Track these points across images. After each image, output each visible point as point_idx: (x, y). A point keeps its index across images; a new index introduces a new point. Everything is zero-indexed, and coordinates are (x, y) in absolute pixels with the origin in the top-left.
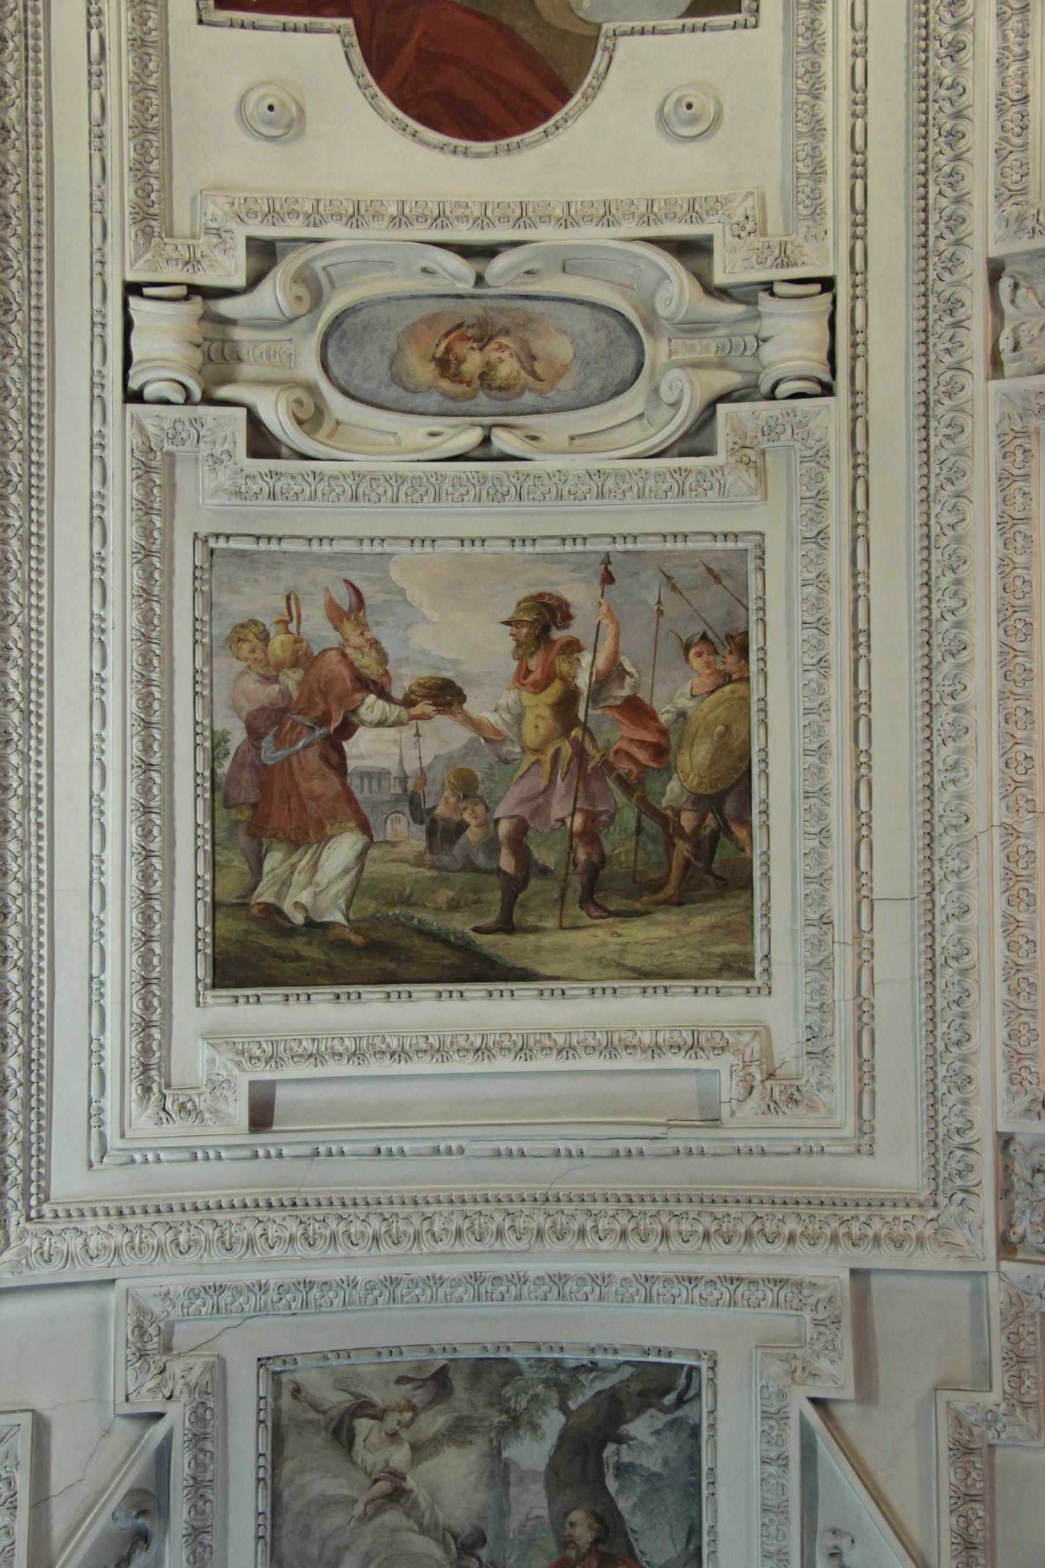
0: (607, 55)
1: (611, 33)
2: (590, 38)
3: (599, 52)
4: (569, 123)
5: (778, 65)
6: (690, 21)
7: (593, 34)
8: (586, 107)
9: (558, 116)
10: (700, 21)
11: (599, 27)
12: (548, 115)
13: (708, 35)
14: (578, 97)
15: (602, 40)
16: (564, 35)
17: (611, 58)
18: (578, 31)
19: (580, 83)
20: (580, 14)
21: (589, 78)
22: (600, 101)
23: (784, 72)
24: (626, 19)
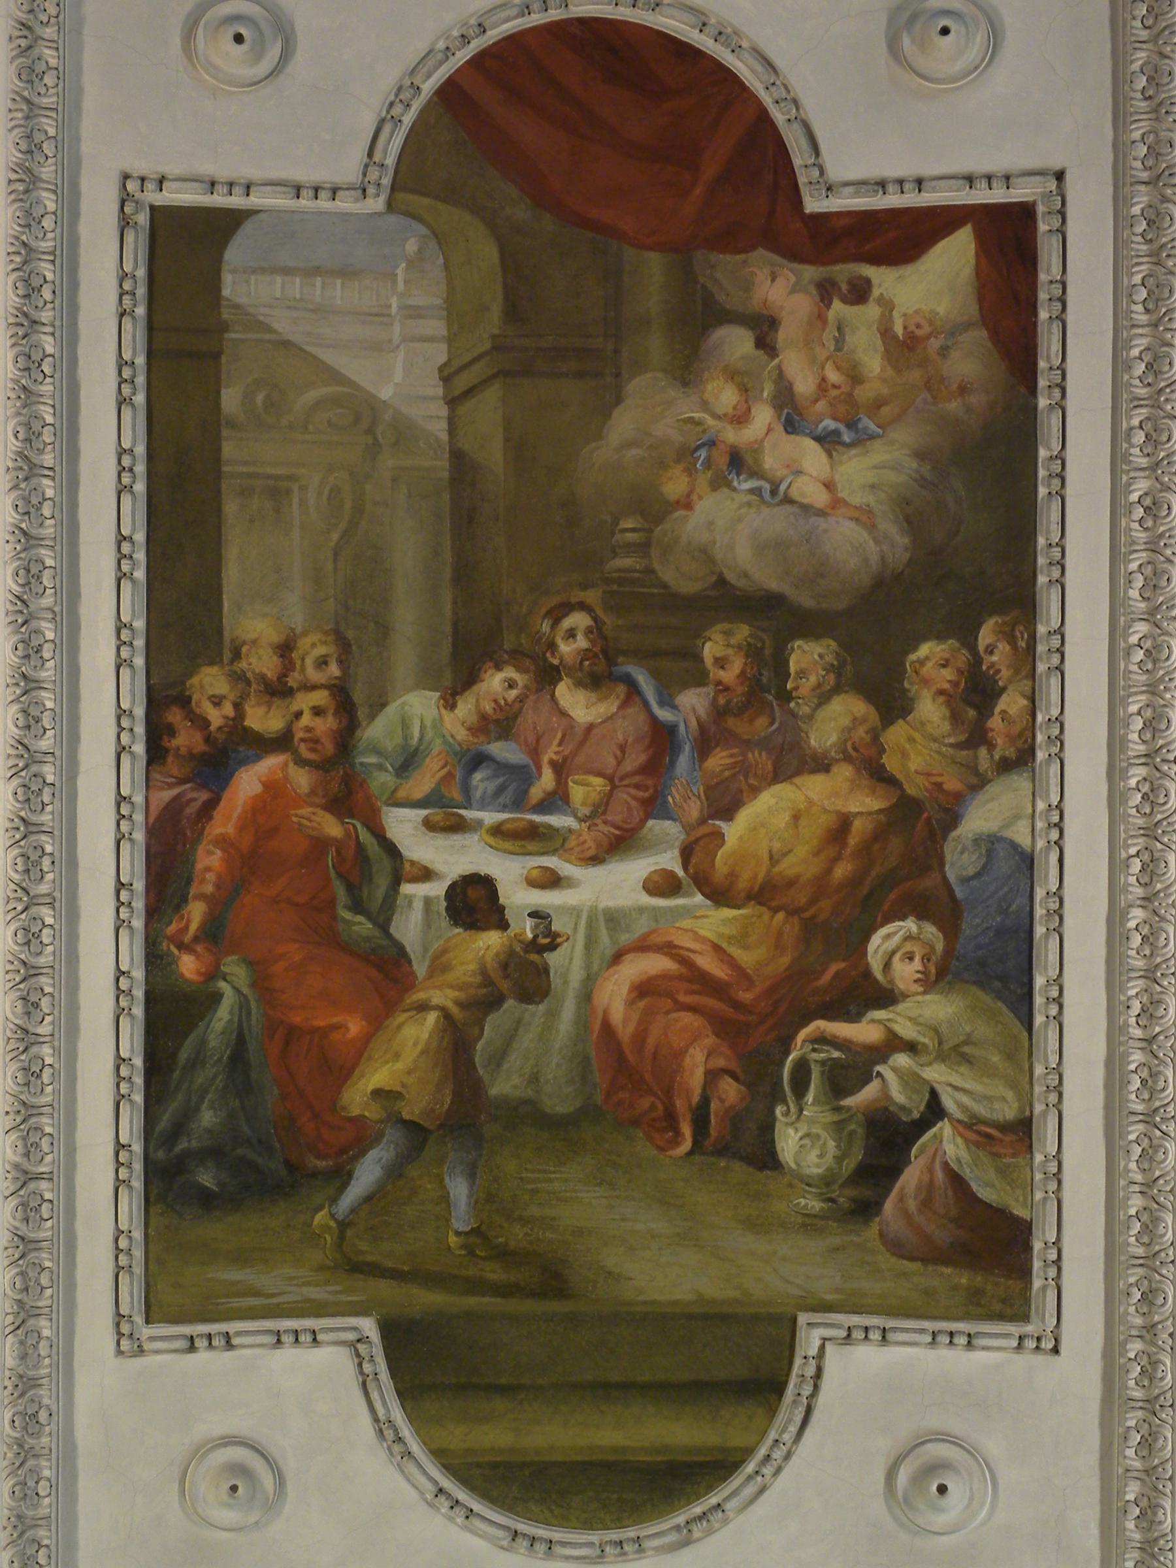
0: (377, 157)
1: (371, 190)
2: (405, 189)
3: (390, 161)
4: (441, 45)
5: (88, 104)
6: (237, 201)
7: (400, 196)
8: (413, 72)
9: (463, 56)
10: (219, 200)
11: (390, 206)
12: (478, 61)
13: (208, 168)
14: (429, 86)
15: (386, 181)
16: (450, 194)
17: (370, 154)
18: (426, 201)
19: (423, 112)
20: (423, 230)
21: (408, 119)
22: (389, 77)
23: (80, 91)
24: (345, 216)
